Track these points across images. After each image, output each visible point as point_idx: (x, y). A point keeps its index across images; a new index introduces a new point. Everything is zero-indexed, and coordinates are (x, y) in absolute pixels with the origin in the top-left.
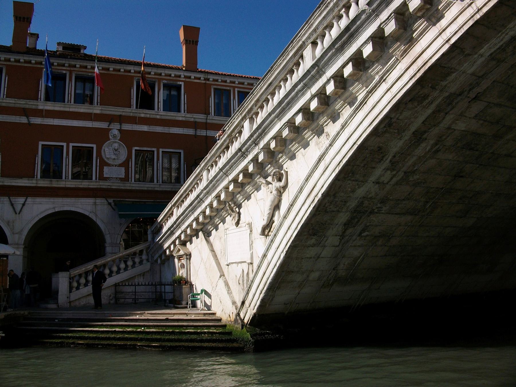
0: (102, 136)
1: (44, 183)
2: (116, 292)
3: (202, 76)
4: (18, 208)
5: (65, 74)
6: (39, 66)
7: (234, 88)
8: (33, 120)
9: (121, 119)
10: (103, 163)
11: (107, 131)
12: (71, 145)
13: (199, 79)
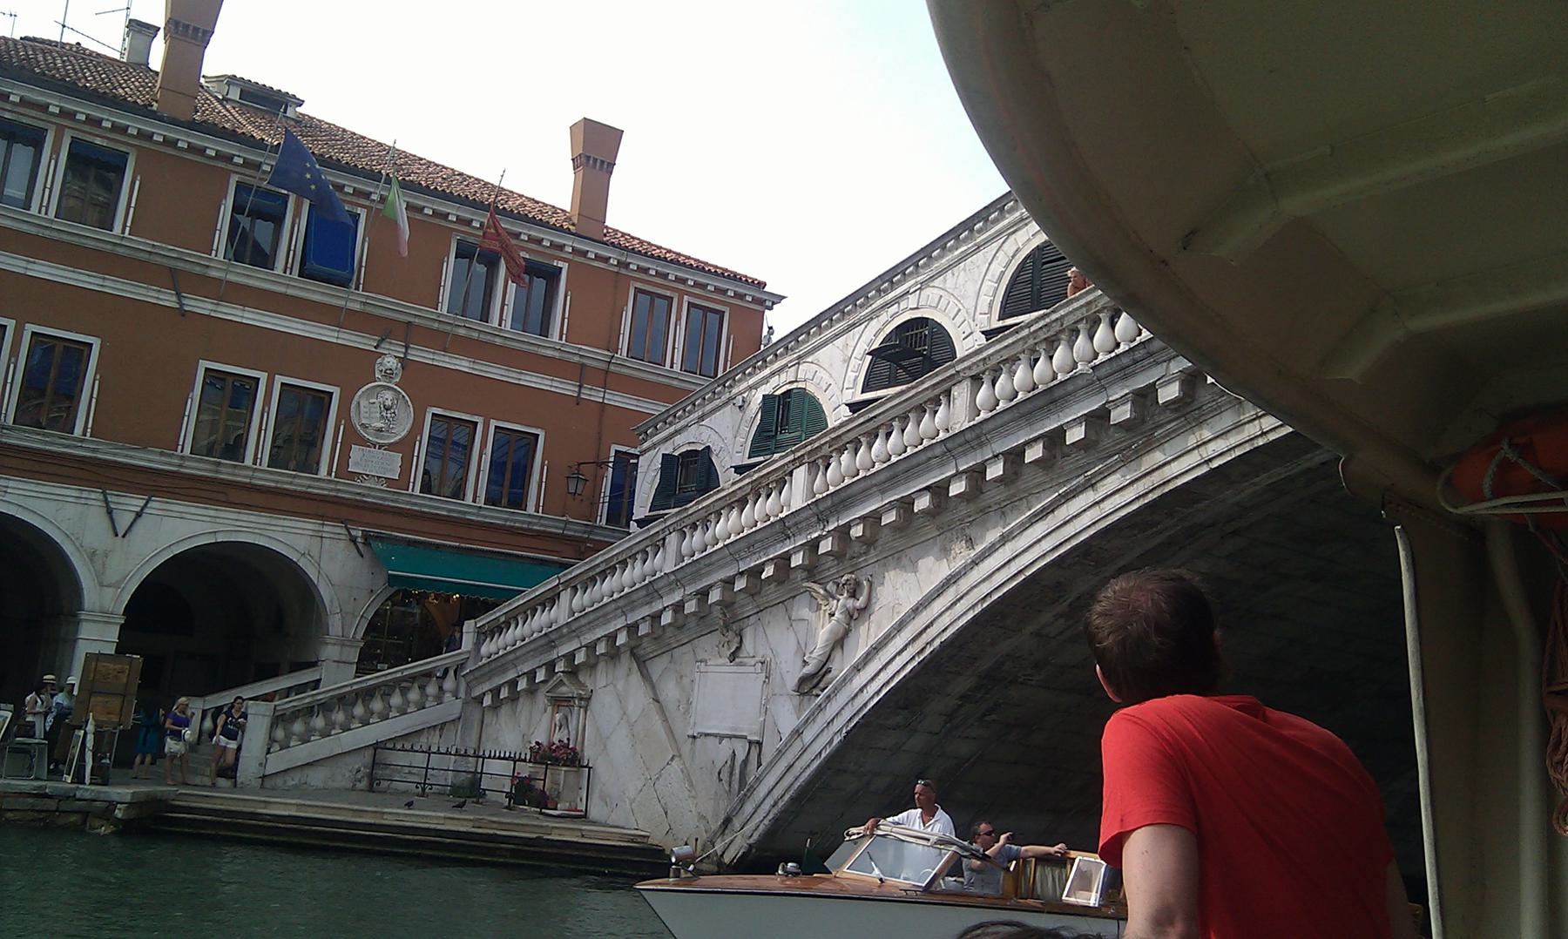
0: (358, 369)
1: (199, 467)
2: (374, 764)
3: (614, 256)
4: (124, 521)
6: (221, 165)
7: (682, 293)
8: (192, 303)
9: (408, 333)
10: (353, 437)
12: (279, 379)
13: (607, 260)
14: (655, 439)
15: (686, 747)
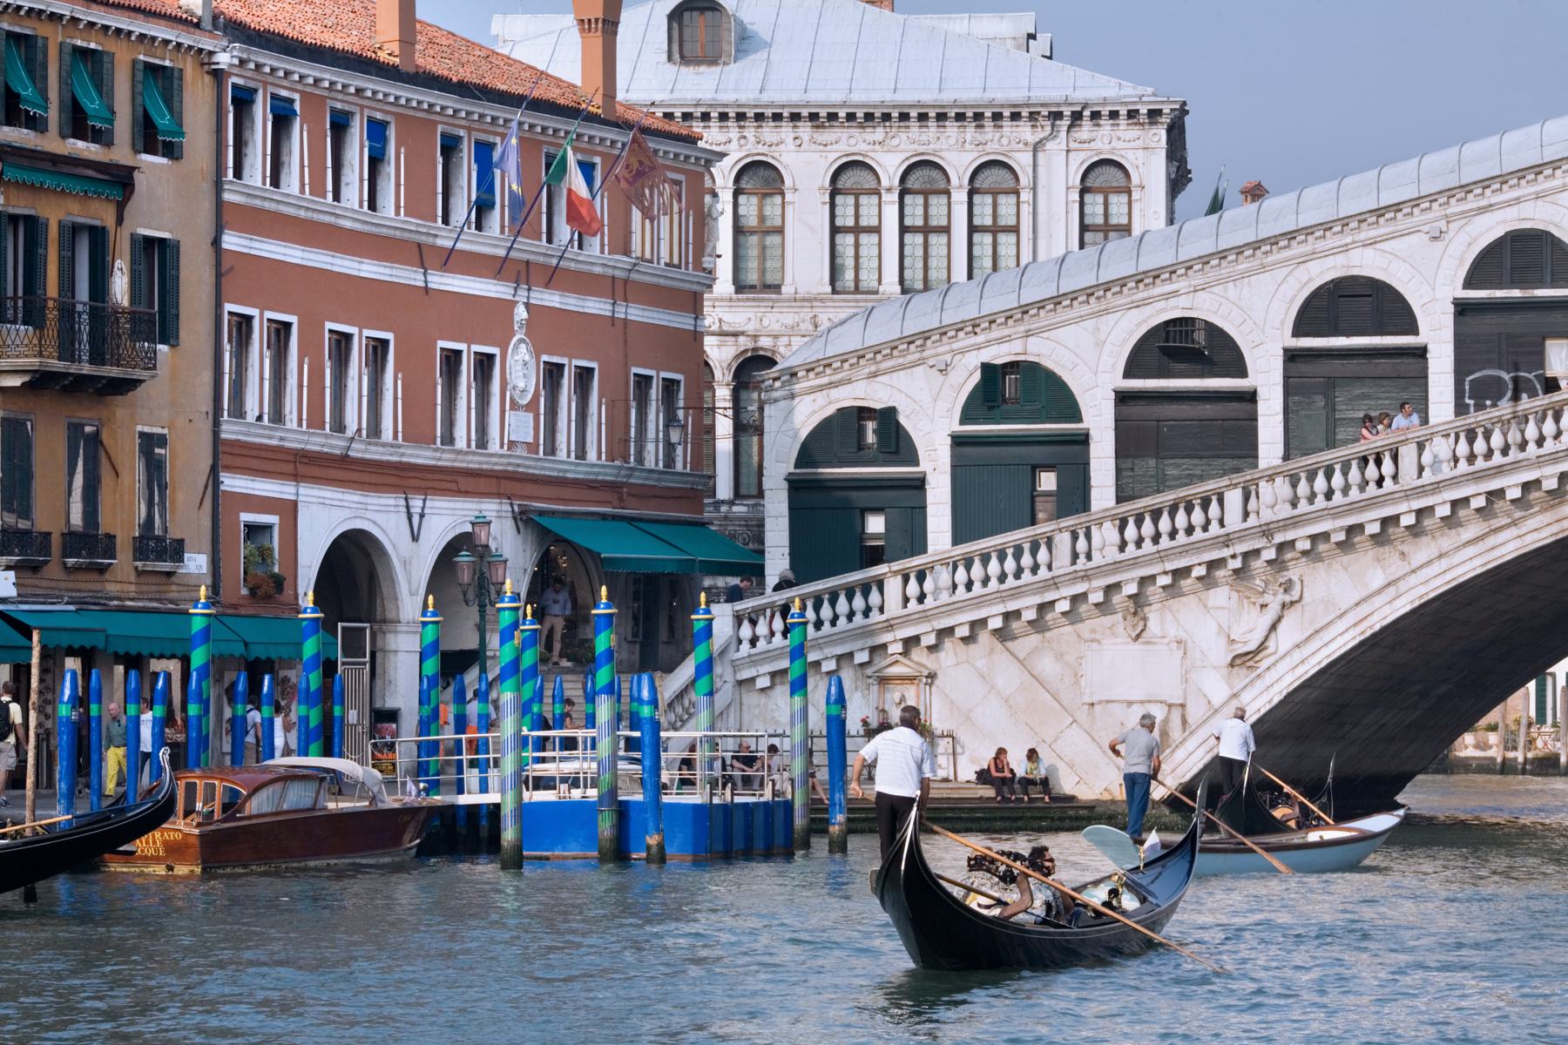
5: (459, 139)
11: (511, 305)
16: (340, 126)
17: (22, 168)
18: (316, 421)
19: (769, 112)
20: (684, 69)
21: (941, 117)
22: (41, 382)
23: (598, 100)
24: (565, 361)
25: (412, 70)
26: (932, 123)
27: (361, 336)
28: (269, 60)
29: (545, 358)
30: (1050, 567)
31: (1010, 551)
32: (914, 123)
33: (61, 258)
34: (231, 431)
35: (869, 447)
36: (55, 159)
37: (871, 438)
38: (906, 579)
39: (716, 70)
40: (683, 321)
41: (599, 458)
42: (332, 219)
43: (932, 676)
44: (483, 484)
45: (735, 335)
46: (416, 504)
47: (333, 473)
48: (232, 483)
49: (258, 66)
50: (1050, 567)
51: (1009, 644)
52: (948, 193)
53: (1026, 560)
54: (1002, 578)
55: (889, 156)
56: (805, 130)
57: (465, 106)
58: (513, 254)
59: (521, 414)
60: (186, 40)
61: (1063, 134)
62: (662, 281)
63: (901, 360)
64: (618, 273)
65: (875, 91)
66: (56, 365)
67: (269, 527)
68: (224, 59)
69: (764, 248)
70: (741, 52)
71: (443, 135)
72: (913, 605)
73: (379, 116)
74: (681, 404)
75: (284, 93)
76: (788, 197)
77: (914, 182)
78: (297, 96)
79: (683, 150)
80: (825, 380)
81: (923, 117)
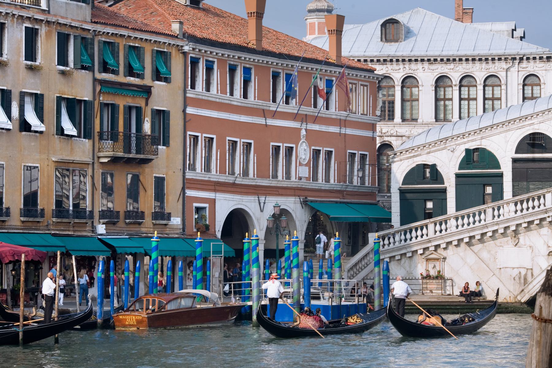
5: (279, 73)
10: (301, 164)
14: (402, 157)
15: (497, 272)
16: (233, 70)
17: (108, 87)
18: (222, 171)
19: (413, 59)
20: (386, 44)
21: (474, 60)
22: (115, 160)
23: (334, 58)
24: (321, 148)
25: (261, 50)
26: (470, 62)
27: (240, 142)
28: (204, 48)
29: (313, 148)
30: (485, 220)
31: (471, 215)
32: (464, 62)
33: (124, 118)
34: (189, 175)
35: (427, 178)
36: (121, 84)
37: (428, 175)
38: (436, 225)
39: (397, 44)
40: (369, 134)
41: (335, 182)
42: (229, 102)
43: (445, 259)
44: (289, 192)
45: (402, 136)
46: (262, 199)
47: (230, 189)
48: (190, 193)
49: (200, 50)
50: (485, 220)
51: (472, 247)
52: (476, 86)
53: (477, 218)
54: (469, 224)
55: (455, 73)
56: (426, 65)
57: (280, 62)
58: (300, 112)
59: (304, 167)
60: (172, 42)
61: (517, 65)
62: (360, 120)
63: (438, 148)
64: (342, 118)
65: (450, 51)
66: (121, 154)
67: (205, 208)
68: (186, 48)
69: (412, 106)
70: (406, 37)
71: (273, 72)
72: (438, 234)
73: (248, 66)
74: (367, 163)
75: (210, 59)
76: (420, 88)
77: (464, 82)
78: (216, 60)
79: (367, 74)
80: (412, 155)
81: (467, 60)
